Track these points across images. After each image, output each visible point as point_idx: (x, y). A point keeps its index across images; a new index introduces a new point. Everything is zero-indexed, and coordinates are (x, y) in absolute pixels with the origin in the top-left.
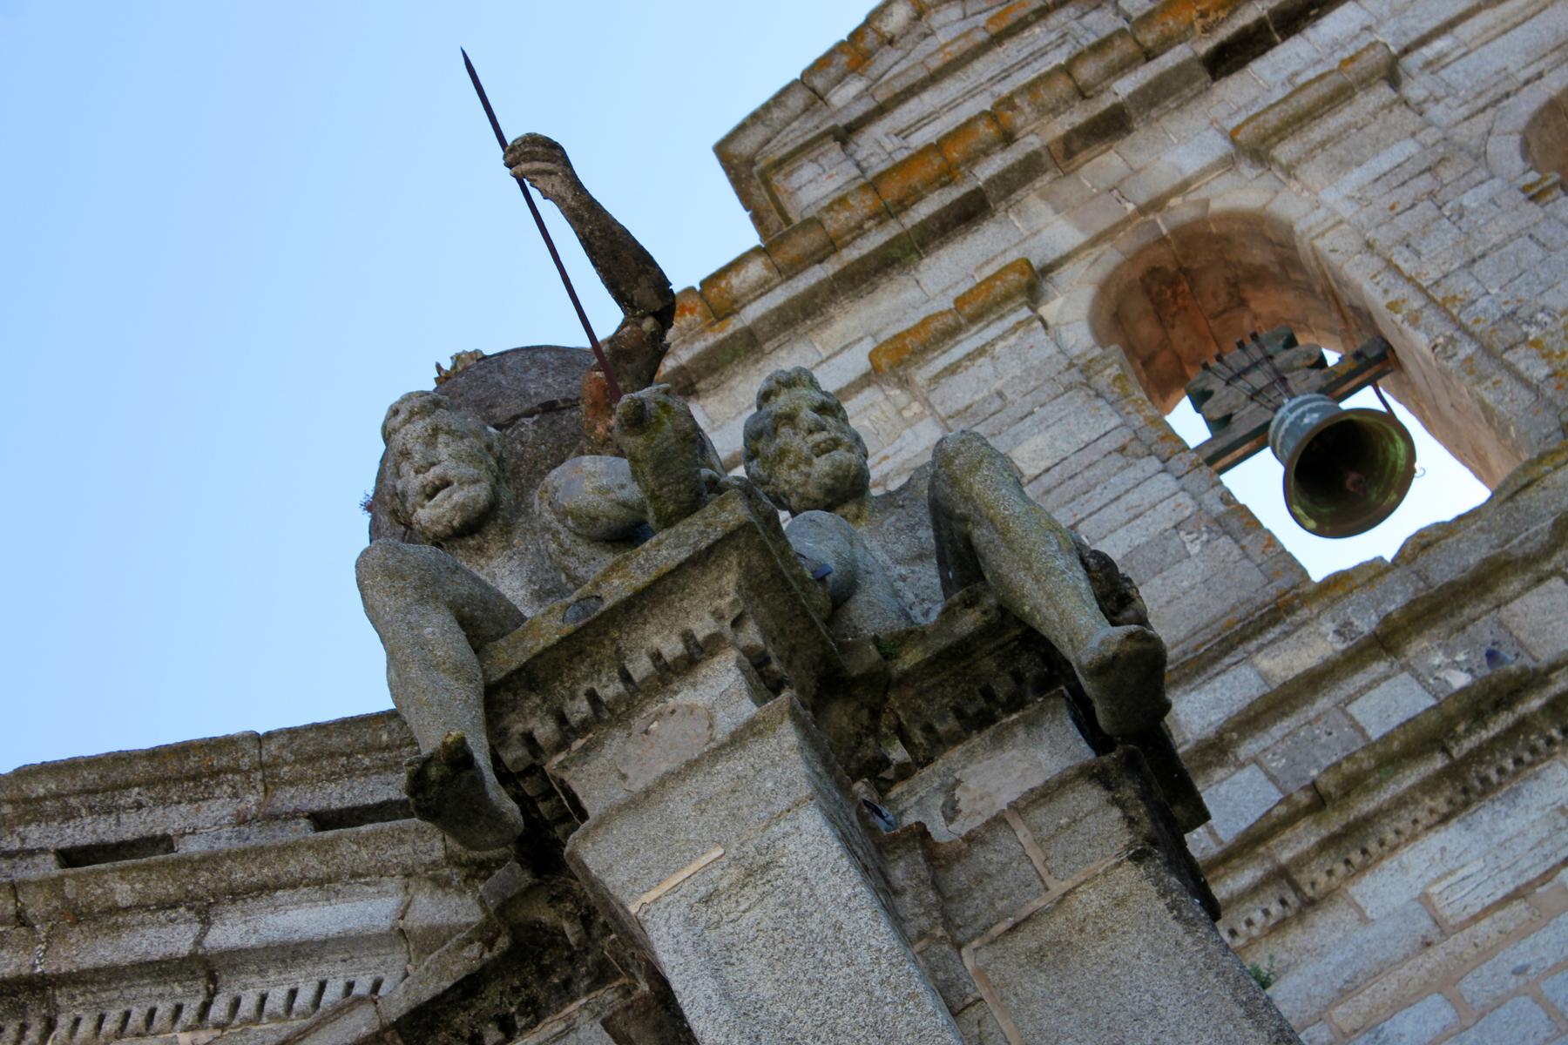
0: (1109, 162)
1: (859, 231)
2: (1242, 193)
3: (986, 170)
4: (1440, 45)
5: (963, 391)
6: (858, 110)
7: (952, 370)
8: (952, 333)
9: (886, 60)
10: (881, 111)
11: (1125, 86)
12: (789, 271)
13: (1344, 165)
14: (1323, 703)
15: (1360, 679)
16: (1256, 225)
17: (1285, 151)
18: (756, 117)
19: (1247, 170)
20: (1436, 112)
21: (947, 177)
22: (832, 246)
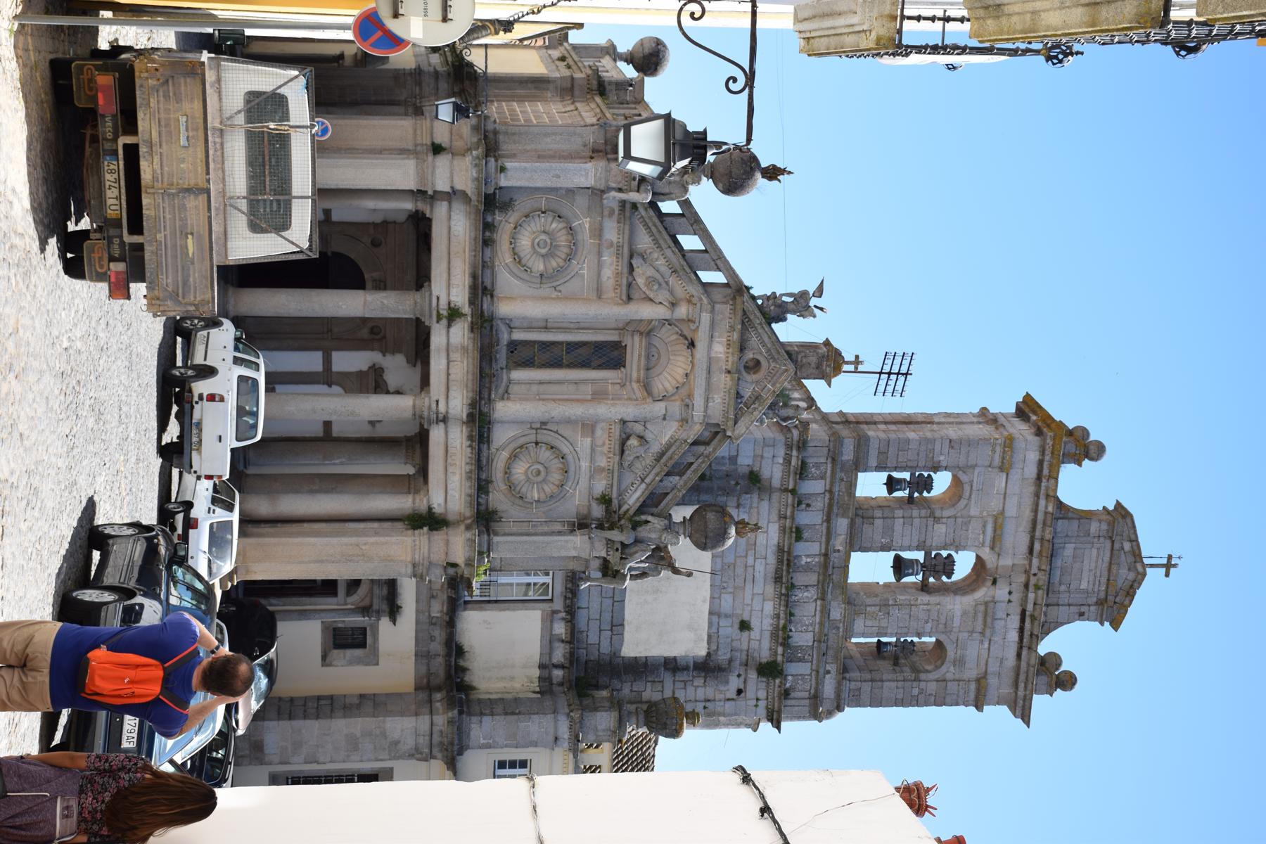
0: (1022, 579)
1: (1043, 531)
2: (981, 594)
3: (1035, 561)
4: (986, 645)
5: (975, 526)
6: (1117, 546)
7: (984, 526)
8: (995, 531)
9: (1131, 559)
10: (1112, 549)
11: (1031, 596)
12: (1046, 513)
13: (964, 613)
14: (824, 539)
15: (823, 546)
16: (973, 590)
17: (982, 608)
18: (1134, 527)
19: (987, 599)
20: (966, 635)
21: (1041, 552)
22: (1044, 524)
